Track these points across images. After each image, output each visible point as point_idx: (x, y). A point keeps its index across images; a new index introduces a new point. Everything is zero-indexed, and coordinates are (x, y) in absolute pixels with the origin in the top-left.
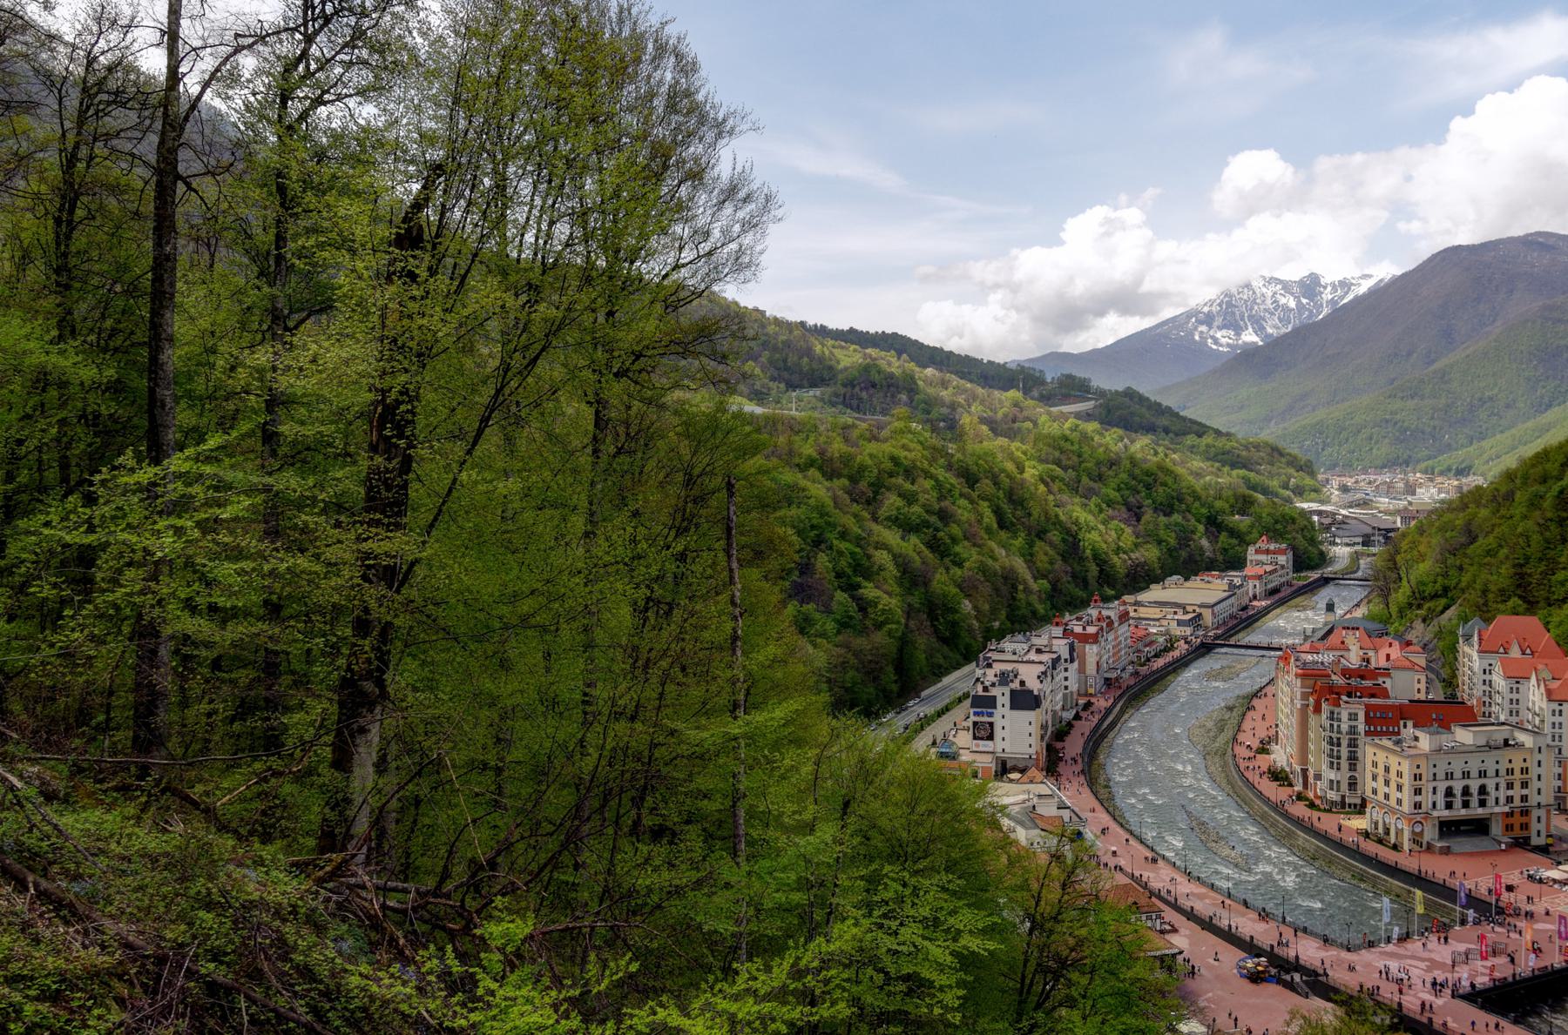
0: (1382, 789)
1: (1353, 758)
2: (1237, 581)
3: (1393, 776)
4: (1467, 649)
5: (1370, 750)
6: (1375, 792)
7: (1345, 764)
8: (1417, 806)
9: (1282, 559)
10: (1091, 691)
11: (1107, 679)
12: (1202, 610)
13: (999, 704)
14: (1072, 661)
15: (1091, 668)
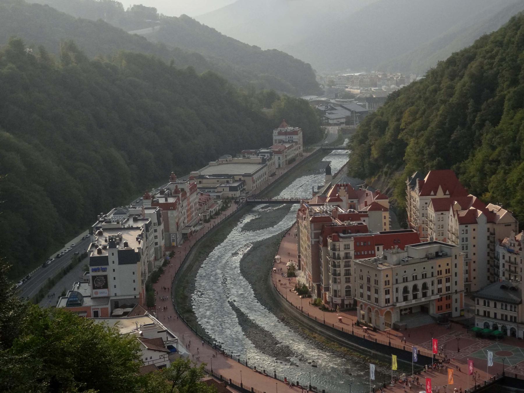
2: (267, 156)
3: (372, 282)
6: (362, 295)
7: (343, 278)
8: (387, 301)
11: (184, 235)
12: (246, 178)
13: (110, 262)
14: (159, 224)
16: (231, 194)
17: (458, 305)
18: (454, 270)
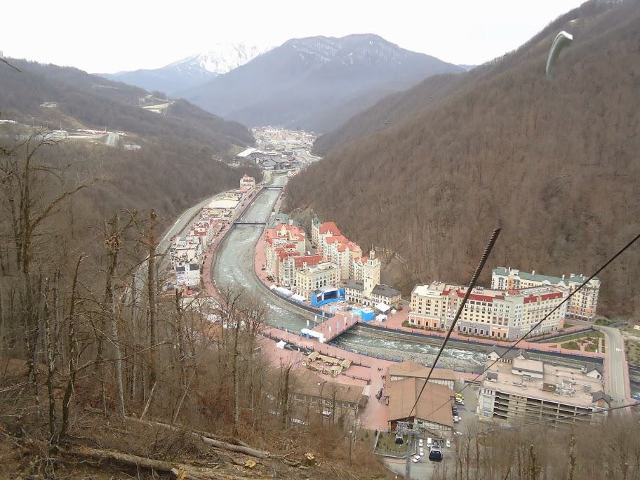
5: (297, 274)
7: (290, 276)
9: (252, 183)
16: (225, 219)
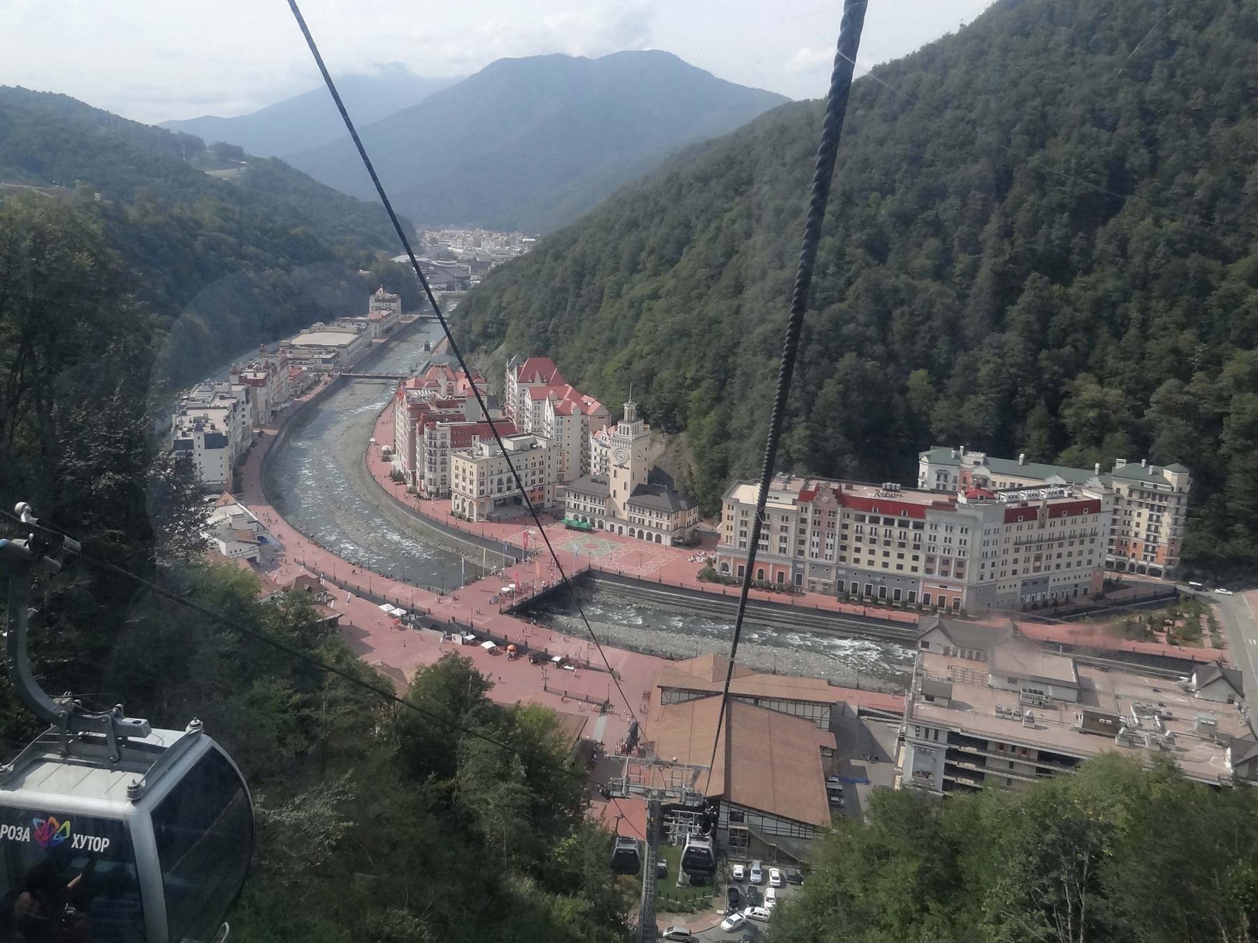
0: (462, 484)
1: (444, 462)
2: (363, 325)
4: (511, 377)
5: (454, 459)
6: (457, 485)
7: (439, 467)
8: (482, 492)
9: (394, 305)
10: (263, 422)
11: (274, 413)
14: (248, 402)
15: (261, 406)
16: (323, 366)
17: (550, 496)
18: (547, 462)
